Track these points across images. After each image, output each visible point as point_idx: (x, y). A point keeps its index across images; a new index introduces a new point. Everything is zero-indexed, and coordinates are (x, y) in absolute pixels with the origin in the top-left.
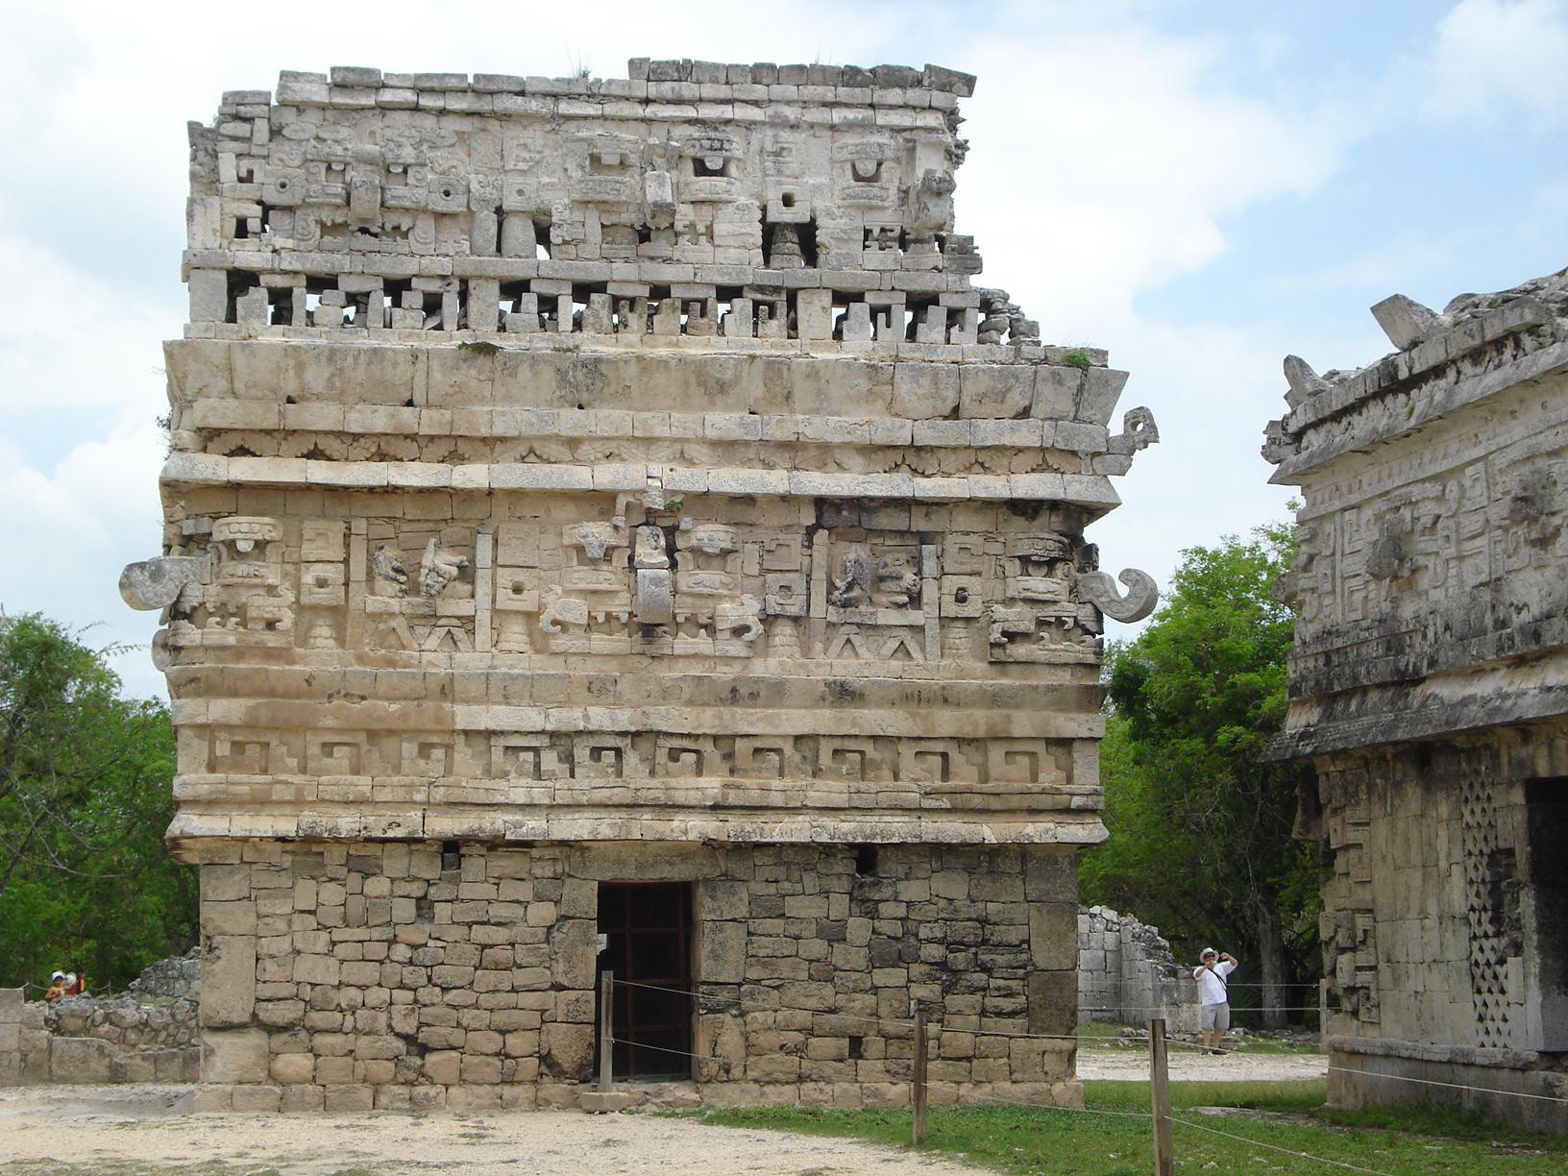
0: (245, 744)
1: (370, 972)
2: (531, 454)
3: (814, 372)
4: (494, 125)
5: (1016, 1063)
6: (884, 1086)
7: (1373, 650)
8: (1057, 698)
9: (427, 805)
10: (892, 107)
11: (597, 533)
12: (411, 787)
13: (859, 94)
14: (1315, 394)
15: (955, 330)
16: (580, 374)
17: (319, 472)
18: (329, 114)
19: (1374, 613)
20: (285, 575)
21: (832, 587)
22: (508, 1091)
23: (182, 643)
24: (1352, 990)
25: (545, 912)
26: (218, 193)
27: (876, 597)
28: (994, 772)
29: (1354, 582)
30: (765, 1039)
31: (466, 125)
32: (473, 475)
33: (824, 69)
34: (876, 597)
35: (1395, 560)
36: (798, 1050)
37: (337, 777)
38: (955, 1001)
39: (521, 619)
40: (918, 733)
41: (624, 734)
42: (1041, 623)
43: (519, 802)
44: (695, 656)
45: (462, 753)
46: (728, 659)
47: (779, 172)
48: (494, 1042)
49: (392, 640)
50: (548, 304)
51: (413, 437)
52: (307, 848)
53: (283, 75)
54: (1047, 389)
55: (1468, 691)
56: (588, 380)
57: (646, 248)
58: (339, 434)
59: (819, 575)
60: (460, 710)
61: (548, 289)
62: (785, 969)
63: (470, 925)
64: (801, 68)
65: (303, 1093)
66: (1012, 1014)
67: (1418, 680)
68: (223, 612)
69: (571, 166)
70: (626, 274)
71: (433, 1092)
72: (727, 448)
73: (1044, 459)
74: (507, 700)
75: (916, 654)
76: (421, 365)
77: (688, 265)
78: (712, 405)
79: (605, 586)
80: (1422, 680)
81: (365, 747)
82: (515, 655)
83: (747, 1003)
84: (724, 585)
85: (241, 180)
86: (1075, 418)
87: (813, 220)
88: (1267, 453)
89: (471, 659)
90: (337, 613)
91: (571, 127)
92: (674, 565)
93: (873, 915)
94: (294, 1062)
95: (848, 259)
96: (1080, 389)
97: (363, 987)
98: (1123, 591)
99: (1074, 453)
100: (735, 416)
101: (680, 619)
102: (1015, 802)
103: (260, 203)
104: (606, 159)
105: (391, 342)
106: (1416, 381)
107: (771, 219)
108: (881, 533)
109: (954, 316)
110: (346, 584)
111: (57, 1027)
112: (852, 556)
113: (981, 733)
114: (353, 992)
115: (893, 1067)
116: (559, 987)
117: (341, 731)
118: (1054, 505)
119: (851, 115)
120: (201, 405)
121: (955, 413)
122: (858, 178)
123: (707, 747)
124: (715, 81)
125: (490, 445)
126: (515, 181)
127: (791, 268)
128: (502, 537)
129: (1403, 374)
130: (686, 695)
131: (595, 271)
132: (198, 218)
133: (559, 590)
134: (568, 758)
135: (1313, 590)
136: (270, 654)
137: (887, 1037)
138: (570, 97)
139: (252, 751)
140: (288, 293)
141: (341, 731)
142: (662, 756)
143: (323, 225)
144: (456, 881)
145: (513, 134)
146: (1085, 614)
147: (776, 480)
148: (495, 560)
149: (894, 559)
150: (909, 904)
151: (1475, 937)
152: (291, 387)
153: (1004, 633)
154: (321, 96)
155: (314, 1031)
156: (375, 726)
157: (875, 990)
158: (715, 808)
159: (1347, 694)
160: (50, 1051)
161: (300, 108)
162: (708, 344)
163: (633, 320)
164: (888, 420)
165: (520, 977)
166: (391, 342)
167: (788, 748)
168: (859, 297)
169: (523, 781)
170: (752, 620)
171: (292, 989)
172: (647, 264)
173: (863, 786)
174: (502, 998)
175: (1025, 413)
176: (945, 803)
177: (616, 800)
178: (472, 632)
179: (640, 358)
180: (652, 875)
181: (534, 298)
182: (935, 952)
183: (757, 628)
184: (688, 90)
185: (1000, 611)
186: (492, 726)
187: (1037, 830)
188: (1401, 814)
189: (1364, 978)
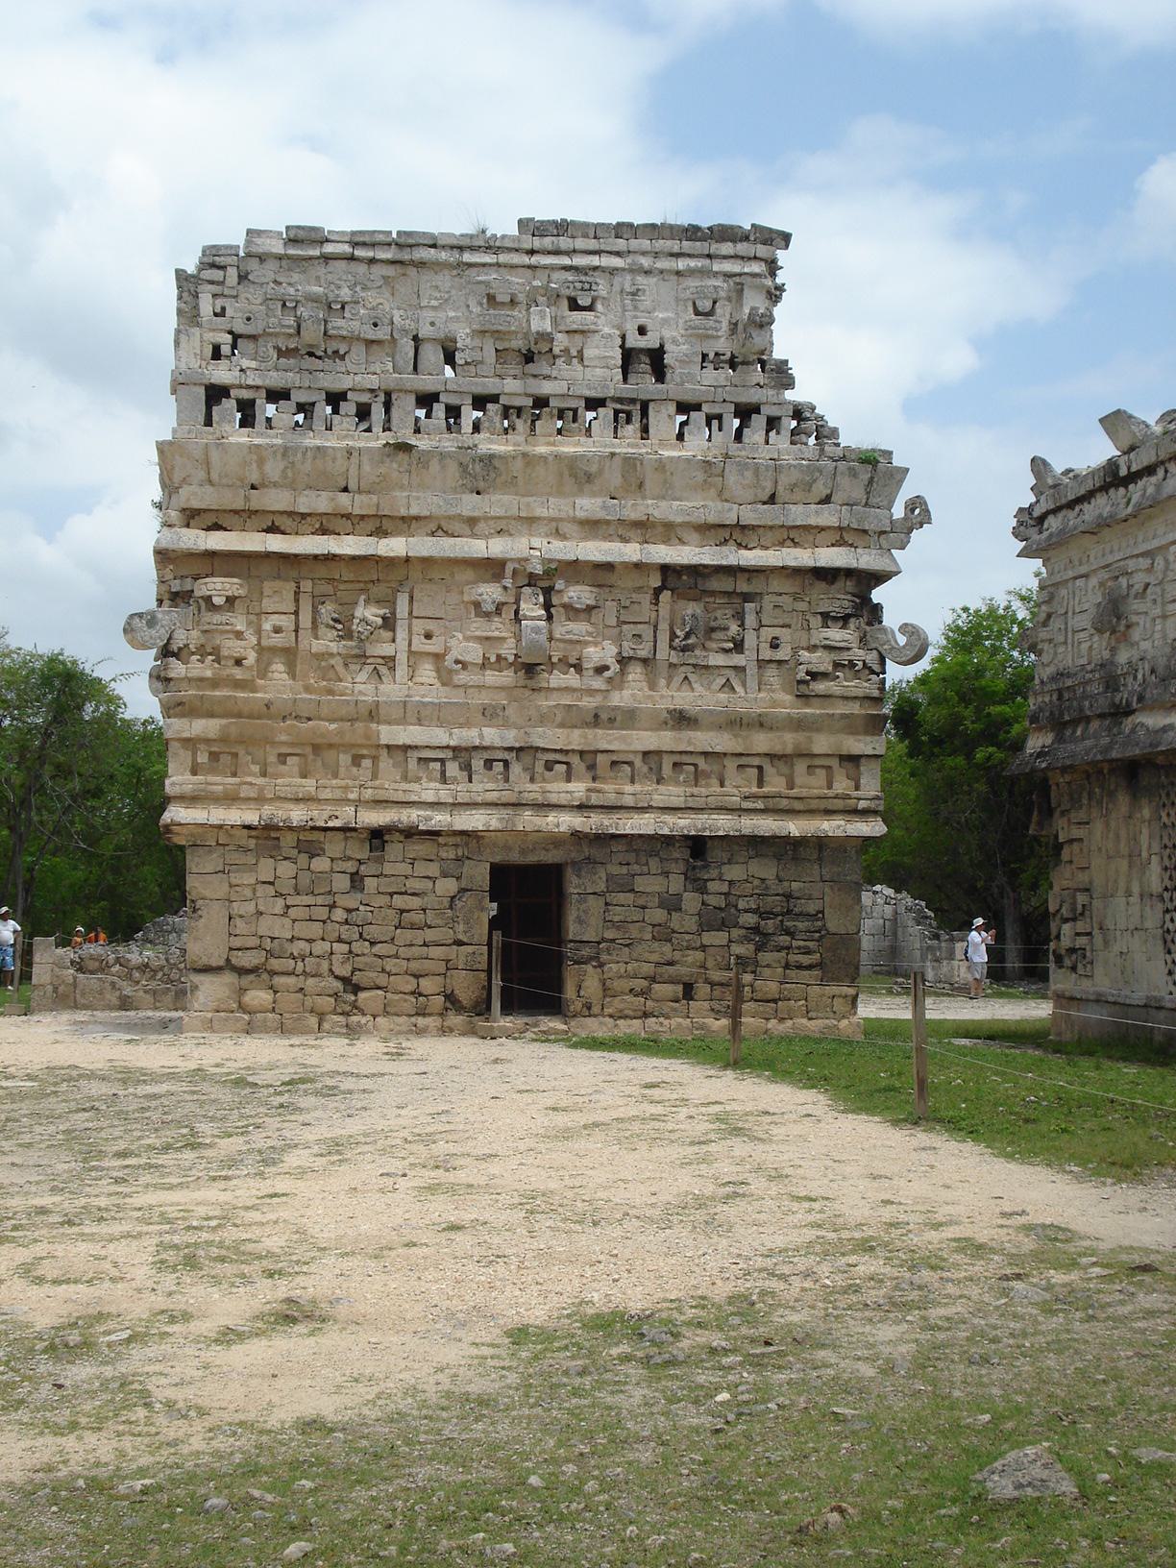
0: (220, 754)
1: (316, 930)
2: (440, 530)
3: (661, 466)
4: (412, 271)
5: (812, 1005)
6: (710, 1021)
7: (1095, 688)
8: (850, 725)
9: (358, 803)
10: (725, 257)
11: (490, 592)
12: (346, 787)
13: (699, 247)
14: (1055, 486)
15: (773, 434)
16: (478, 467)
17: (276, 543)
18: (284, 263)
19: (1096, 659)
20: (249, 624)
21: (673, 636)
22: (421, 1021)
23: (172, 675)
24: (1072, 951)
25: (448, 886)
26: (198, 325)
27: (708, 644)
28: (798, 781)
29: (1082, 635)
30: (618, 985)
31: (390, 271)
32: (394, 546)
33: (671, 227)
34: (708, 644)
35: (1113, 617)
36: (644, 993)
37: (289, 780)
38: (766, 957)
39: (431, 659)
40: (740, 750)
41: (510, 749)
42: (837, 665)
43: (429, 802)
44: (567, 689)
45: (385, 762)
46: (592, 692)
47: (636, 308)
48: (410, 984)
49: (331, 674)
50: (453, 412)
51: (347, 516)
52: (267, 835)
53: (249, 232)
54: (844, 481)
55: (1168, 721)
56: (482, 474)
57: (531, 368)
58: (290, 514)
59: (664, 626)
60: (383, 728)
61: (453, 400)
62: (634, 931)
63: (391, 894)
64: (653, 226)
65: (265, 1020)
66: (810, 967)
67: (1129, 712)
68: (202, 652)
69: (472, 303)
70: (513, 387)
71: (363, 1020)
72: (592, 527)
73: (842, 536)
74: (419, 722)
75: (739, 689)
76: (354, 460)
77: (560, 382)
78: (580, 492)
79: (496, 634)
80: (1133, 712)
81: (311, 757)
82: (426, 688)
83: (604, 957)
84: (590, 634)
85: (216, 315)
86: (866, 505)
87: (662, 346)
88: (1016, 533)
89: (392, 690)
90: (289, 655)
91: (473, 272)
92: (550, 618)
93: (703, 890)
94: (259, 997)
95: (689, 378)
96: (871, 481)
97: (310, 941)
98: (902, 640)
99: (865, 532)
100: (599, 501)
101: (555, 660)
102: (814, 804)
103: (230, 332)
104: (499, 298)
105: (331, 442)
106: (1133, 477)
107: (630, 343)
108: (712, 593)
109: (773, 423)
110: (296, 631)
111: (80, 967)
112: (689, 612)
113: (789, 750)
114: (302, 944)
115: (717, 1007)
116: (459, 943)
117: (292, 744)
118: (849, 573)
119: (693, 263)
120: (184, 492)
121: (772, 500)
122: (697, 313)
123: (575, 760)
124: (586, 236)
125: (407, 523)
126: (428, 315)
127: (644, 384)
128: (417, 595)
129: (1123, 472)
130: (559, 719)
131: (489, 385)
132: (183, 344)
133: (460, 636)
134: (467, 768)
135: (1050, 641)
136: (239, 685)
137: (712, 984)
138: (472, 249)
139: (225, 759)
140: (252, 403)
141: (292, 744)
142: (540, 767)
143: (279, 350)
144: (381, 861)
145: (427, 278)
146: (872, 658)
147: (631, 552)
148: (411, 613)
149: (723, 615)
150: (731, 883)
151: (1168, 911)
152: (254, 477)
153: (808, 673)
154: (278, 248)
155: (273, 973)
156: (319, 741)
157: (703, 948)
158: (582, 807)
159: (1074, 722)
160: (75, 985)
161: (262, 258)
162: (578, 443)
163: (520, 424)
164: (719, 504)
165: (430, 935)
166: (331, 442)
167: (638, 762)
168: (698, 407)
169: (433, 785)
170: (611, 661)
171: (255, 942)
172: (531, 381)
173: (695, 791)
174: (416, 951)
175: (826, 500)
176: (760, 805)
177: (504, 800)
178: (393, 669)
179: (525, 455)
180: (532, 859)
181: (442, 407)
182: (750, 919)
183: (615, 667)
184: (564, 243)
185: (805, 655)
186: (408, 742)
187: (831, 827)
188: (1113, 815)
189: (1082, 941)
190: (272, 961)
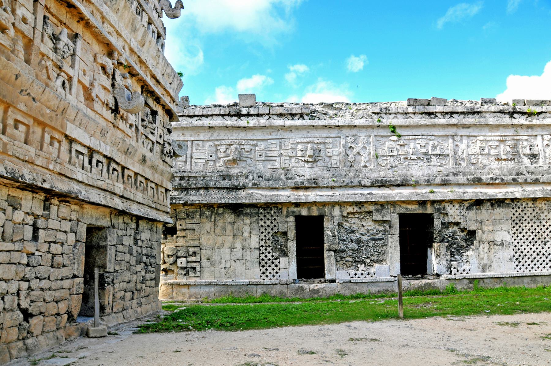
11: (109, 64)
21: (143, 120)
43: (84, 179)
67: (244, 187)
106: (248, 115)
116: (75, 276)
134: (90, 163)
144: (47, 218)
151: (263, 253)
158: (122, 197)
165: (64, 272)
177: (103, 187)
189: (194, 265)
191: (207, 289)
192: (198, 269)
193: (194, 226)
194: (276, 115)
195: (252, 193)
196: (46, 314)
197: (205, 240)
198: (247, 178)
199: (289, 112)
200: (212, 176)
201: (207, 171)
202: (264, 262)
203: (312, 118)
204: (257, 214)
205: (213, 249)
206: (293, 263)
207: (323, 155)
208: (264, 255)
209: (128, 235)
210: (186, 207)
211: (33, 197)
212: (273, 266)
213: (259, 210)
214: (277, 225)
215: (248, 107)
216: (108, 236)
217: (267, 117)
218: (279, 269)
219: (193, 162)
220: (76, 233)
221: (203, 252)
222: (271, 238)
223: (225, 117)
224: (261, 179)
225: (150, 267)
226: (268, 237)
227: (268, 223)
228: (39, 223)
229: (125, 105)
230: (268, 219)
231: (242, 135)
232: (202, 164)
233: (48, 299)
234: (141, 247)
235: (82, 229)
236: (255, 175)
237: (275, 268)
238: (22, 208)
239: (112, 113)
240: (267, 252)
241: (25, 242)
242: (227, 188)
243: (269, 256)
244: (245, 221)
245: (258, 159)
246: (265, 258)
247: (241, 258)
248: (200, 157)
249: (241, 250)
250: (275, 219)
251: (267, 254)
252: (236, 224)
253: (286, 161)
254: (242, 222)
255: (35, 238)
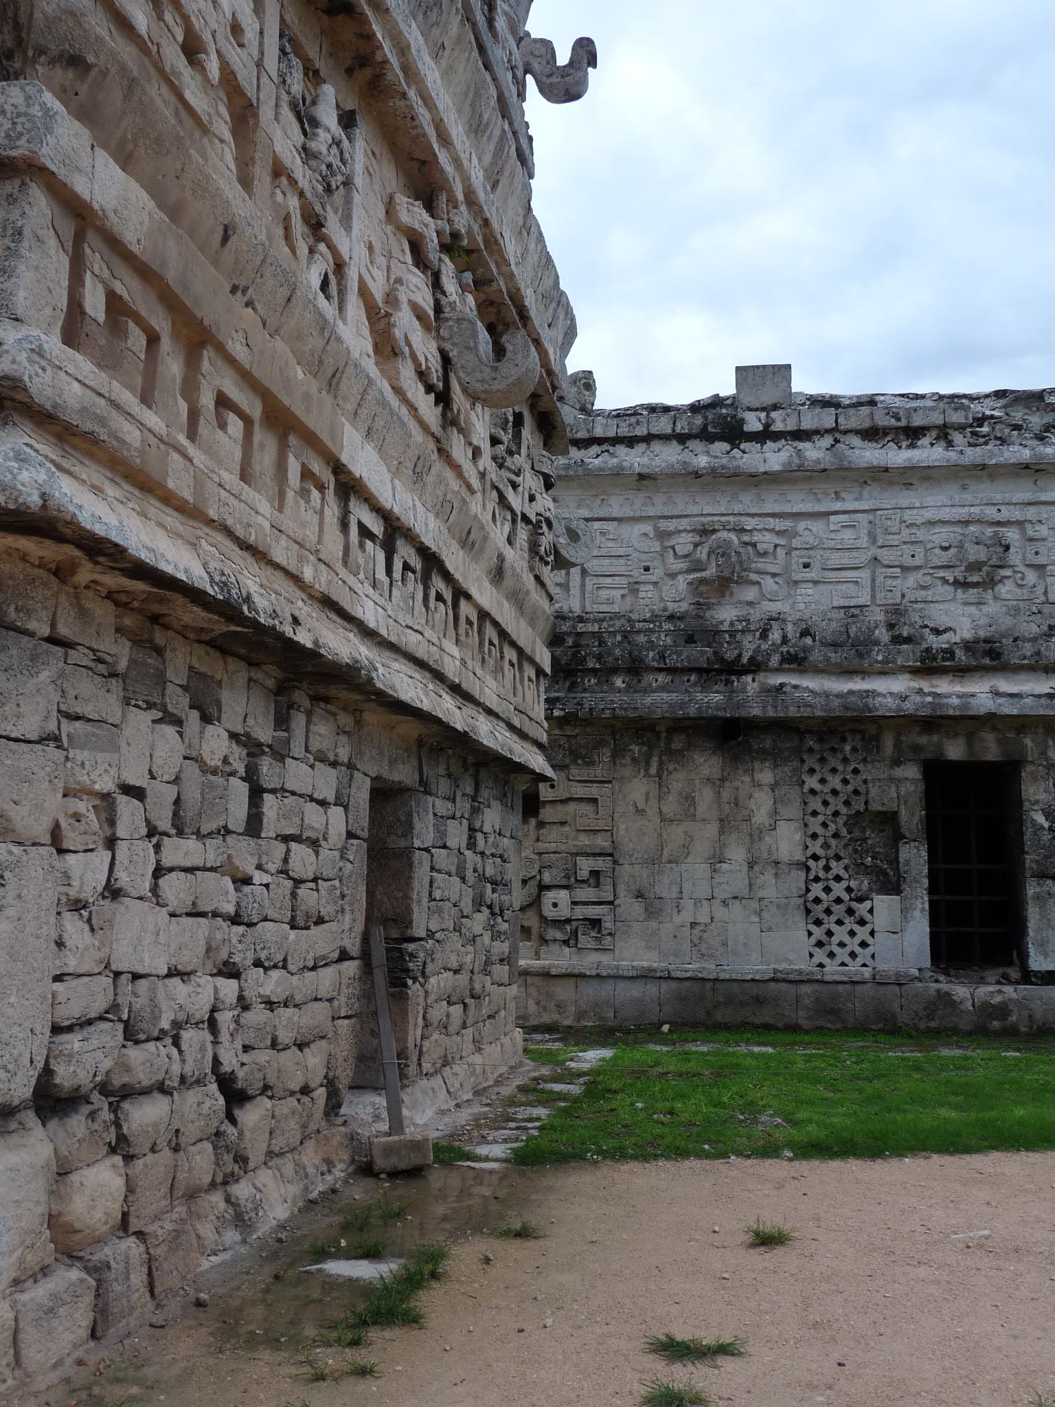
67: (755, 666)
106: (766, 435)
134: (389, 571)
151: (817, 879)
189: (593, 912)
190: (135, 1054)
191: (636, 990)
192: (608, 924)
193: (594, 791)
194: (857, 432)
195: (782, 685)
196: (278, 1092)
197: (634, 834)
198: (764, 635)
199: (903, 423)
200: (650, 630)
201: (635, 616)
202: (820, 908)
203: (977, 439)
204: (798, 754)
205: (653, 861)
206: (917, 914)
207: (1017, 562)
208: (820, 885)
209: (458, 814)
210: (569, 731)
211: (250, 680)
212: (850, 924)
213: (801, 740)
214: (862, 789)
215: (763, 409)
216: (416, 819)
217: (827, 441)
218: (872, 933)
219: (589, 587)
220: (346, 808)
221: (625, 870)
222: (844, 832)
223: (688, 443)
224: (808, 641)
225: (499, 919)
226: (832, 827)
227: (835, 781)
228: (265, 770)
229: (479, 376)
230: (834, 771)
231: (746, 501)
232: (617, 594)
233: (285, 1037)
234: (482, 853)
235: (361, 794)
236: (789, 628)
237: (856, 928)
238: (224, 717)
239: (436, 404)
240: (831, 875)
241: (229, 839)
242: (699, 670)
243: (839, 889)
244: (758, 776)
245: (798, 577)
246: (823, 896)
247: (745, 892)
248: (613, 570)
249: (745, 867)
250: (856, 771)
251: (832, 884)
252: (727, 784)
253: (889, 582)
254: (747, 779)
255: (254, 826)
